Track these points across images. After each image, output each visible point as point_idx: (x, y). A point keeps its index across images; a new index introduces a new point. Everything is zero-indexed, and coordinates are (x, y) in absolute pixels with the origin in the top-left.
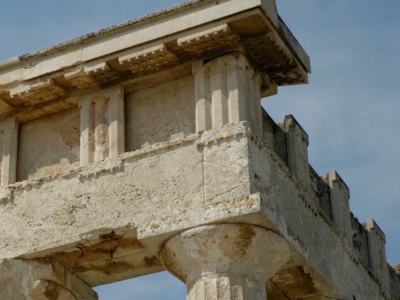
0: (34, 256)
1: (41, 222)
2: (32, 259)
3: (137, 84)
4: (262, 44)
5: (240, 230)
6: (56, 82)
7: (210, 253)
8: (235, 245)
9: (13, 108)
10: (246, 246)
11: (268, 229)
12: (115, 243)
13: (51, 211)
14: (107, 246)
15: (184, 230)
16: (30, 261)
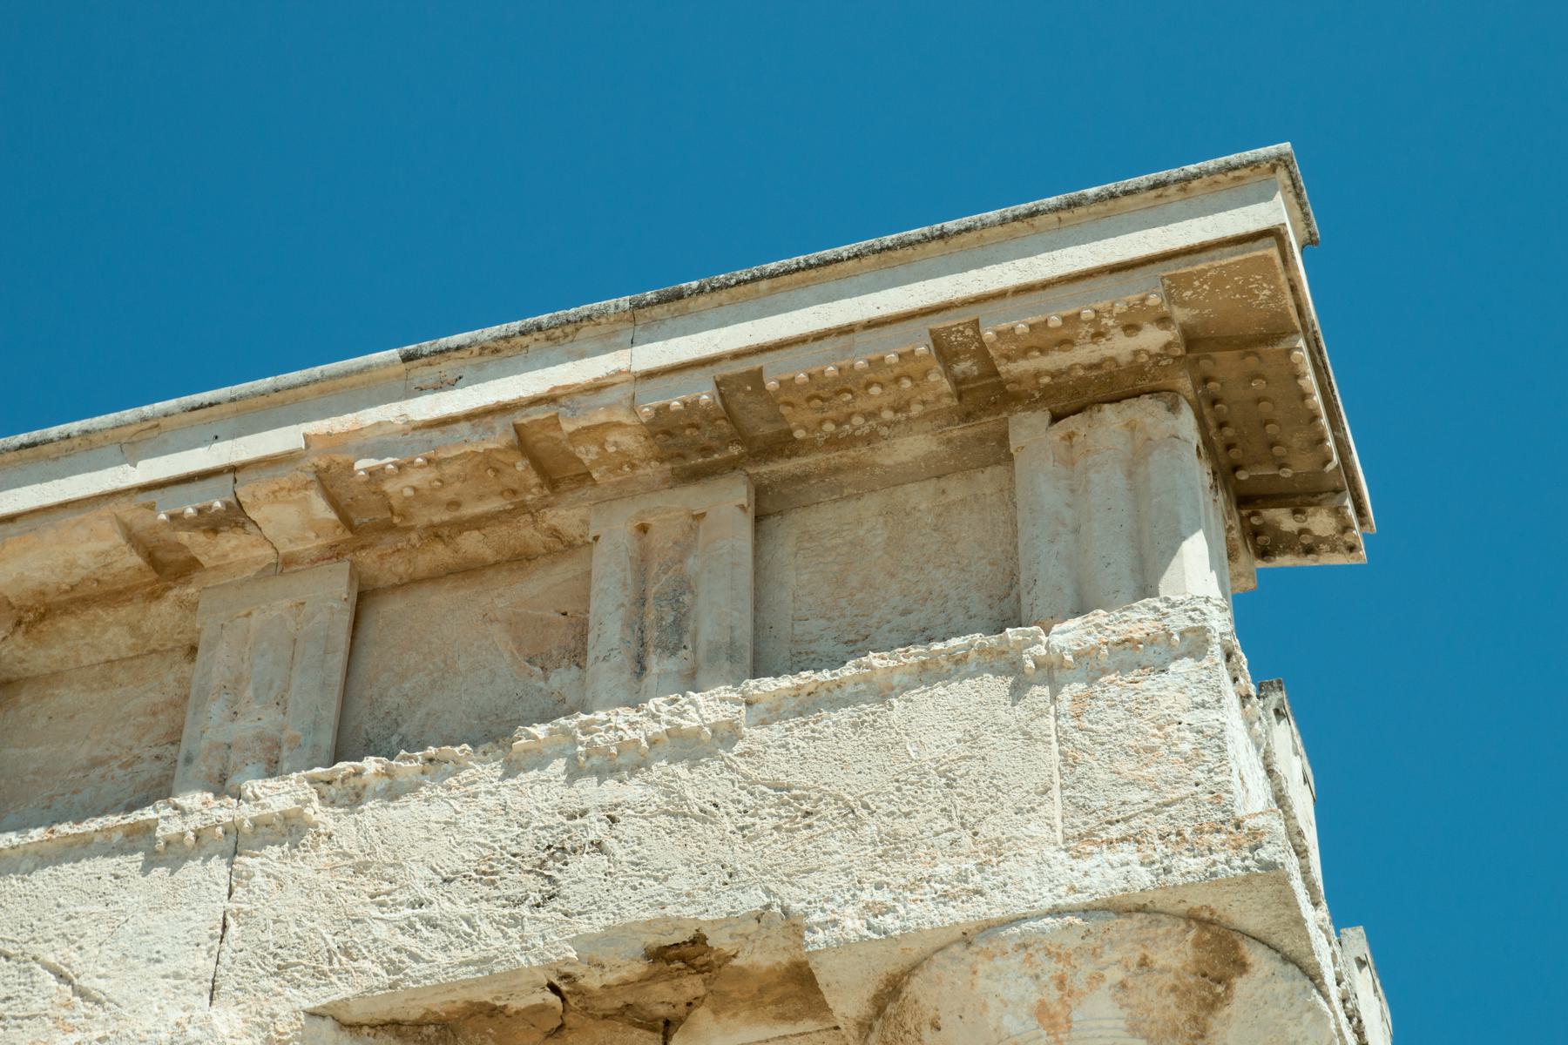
0: (382, 1011)
1: (427, 893)
2: (372, 1027)
3: (804, 478)
4: (1258, 376)
5: (1197, 944)
6: (523, 442)
7: (1076, 1016)
8: (1172, 1000)
9: (348, 535)
10: (1212, 1004)
11: (1287, 959)
12: (693, 985)
13: (463, 858)
14: (662, 997)
15: (989, 928)
16: (366, 1030)
